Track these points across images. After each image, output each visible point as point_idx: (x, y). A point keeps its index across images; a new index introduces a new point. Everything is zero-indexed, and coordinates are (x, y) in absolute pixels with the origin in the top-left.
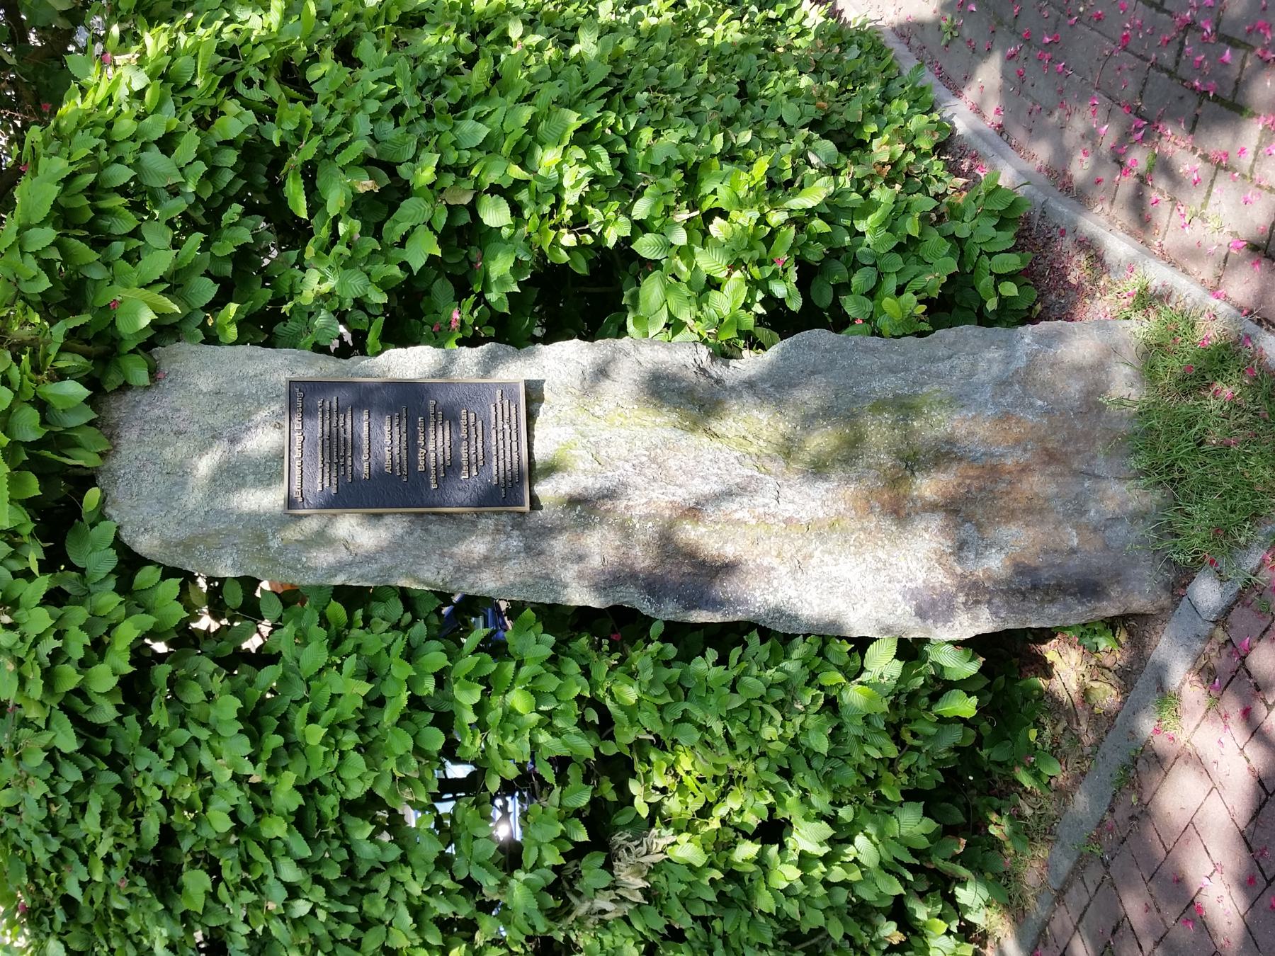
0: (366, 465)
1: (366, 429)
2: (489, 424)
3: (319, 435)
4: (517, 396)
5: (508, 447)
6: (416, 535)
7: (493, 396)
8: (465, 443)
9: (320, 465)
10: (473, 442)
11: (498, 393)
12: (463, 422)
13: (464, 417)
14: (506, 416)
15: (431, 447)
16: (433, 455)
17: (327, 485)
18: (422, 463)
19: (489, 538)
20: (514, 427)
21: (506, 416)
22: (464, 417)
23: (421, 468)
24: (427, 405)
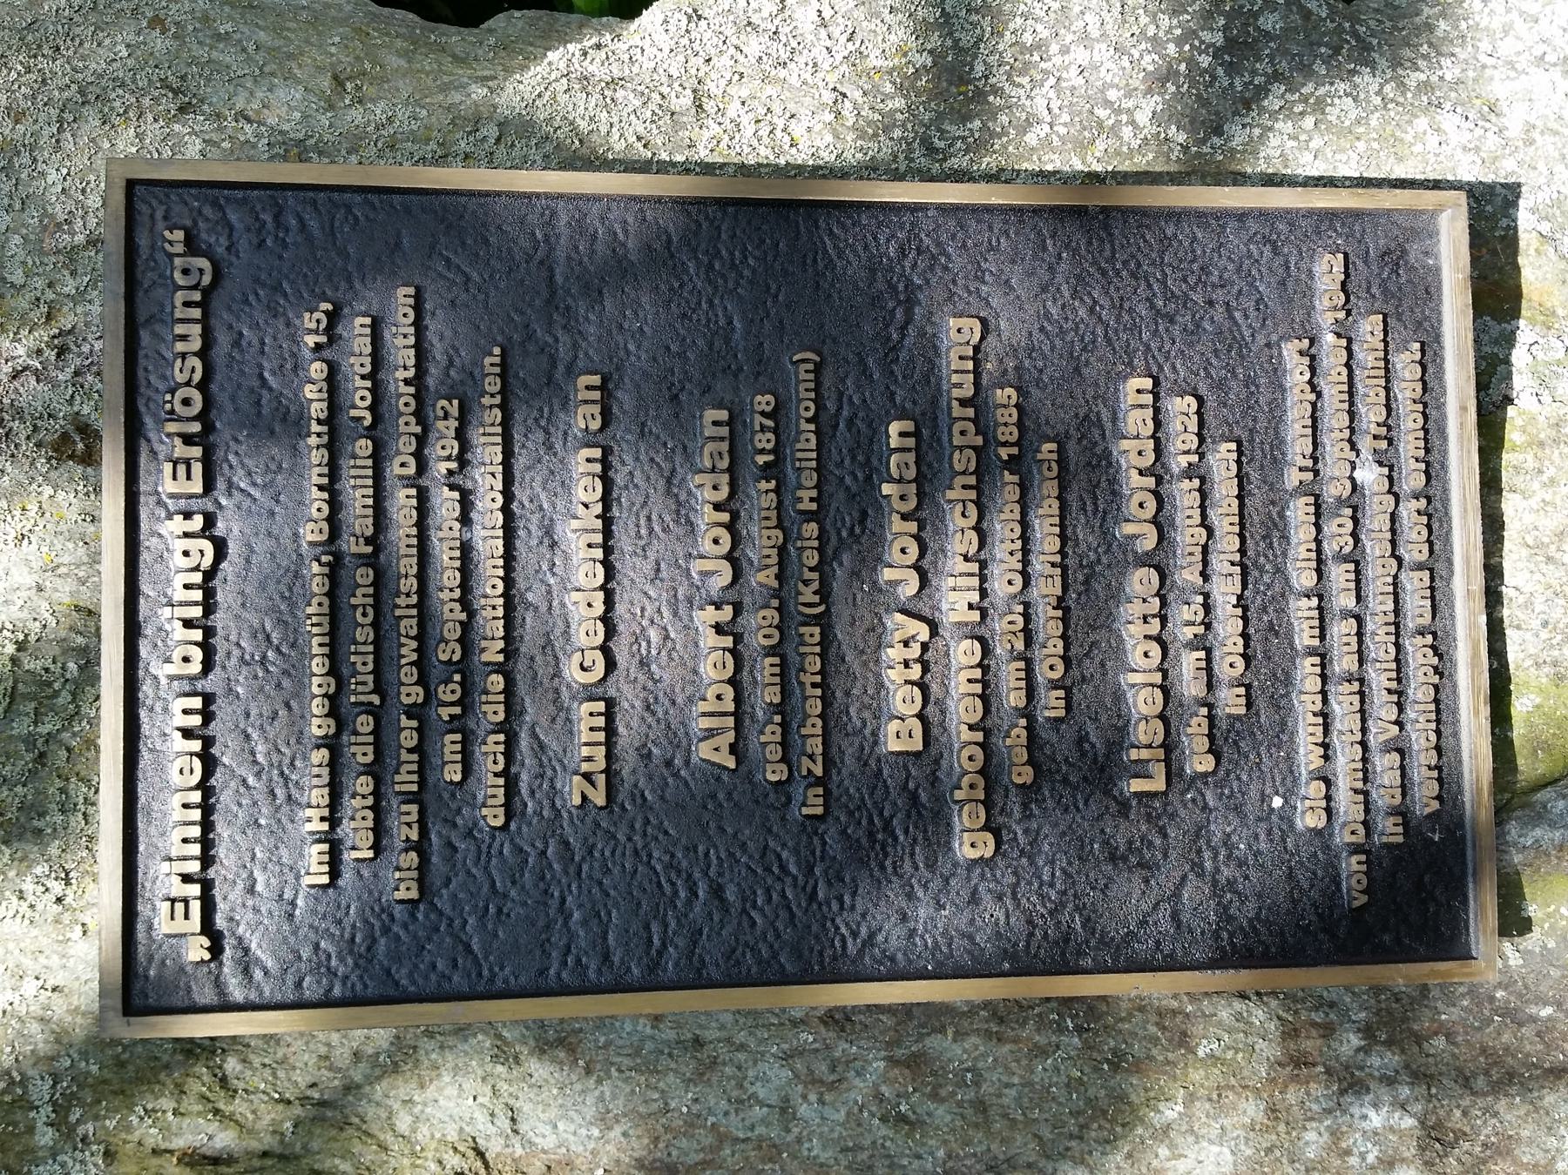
0: (587, 716)
1: (587, 574)
2: (1276, 460)
3: (312, 533)
4: (1429, 292)
5: (1380, 605)
6: (859, 1089)
7: (1296, 291)
8: (1141, 581)
9: (318, 727)
10: (1188, 575)
11: (1327, 272)
12: (1132, 453)
13: (1137, 421)
14: (1372, 415)
15: (955, 603)
16: (964, 653)
17: (358, 848)
18: (905, 701)
19: (1252, 1109)
20: (1413, 479)
21: (1372, 415)
22: (1137, 421)
23: (899, 737)
24: (931, 349)
